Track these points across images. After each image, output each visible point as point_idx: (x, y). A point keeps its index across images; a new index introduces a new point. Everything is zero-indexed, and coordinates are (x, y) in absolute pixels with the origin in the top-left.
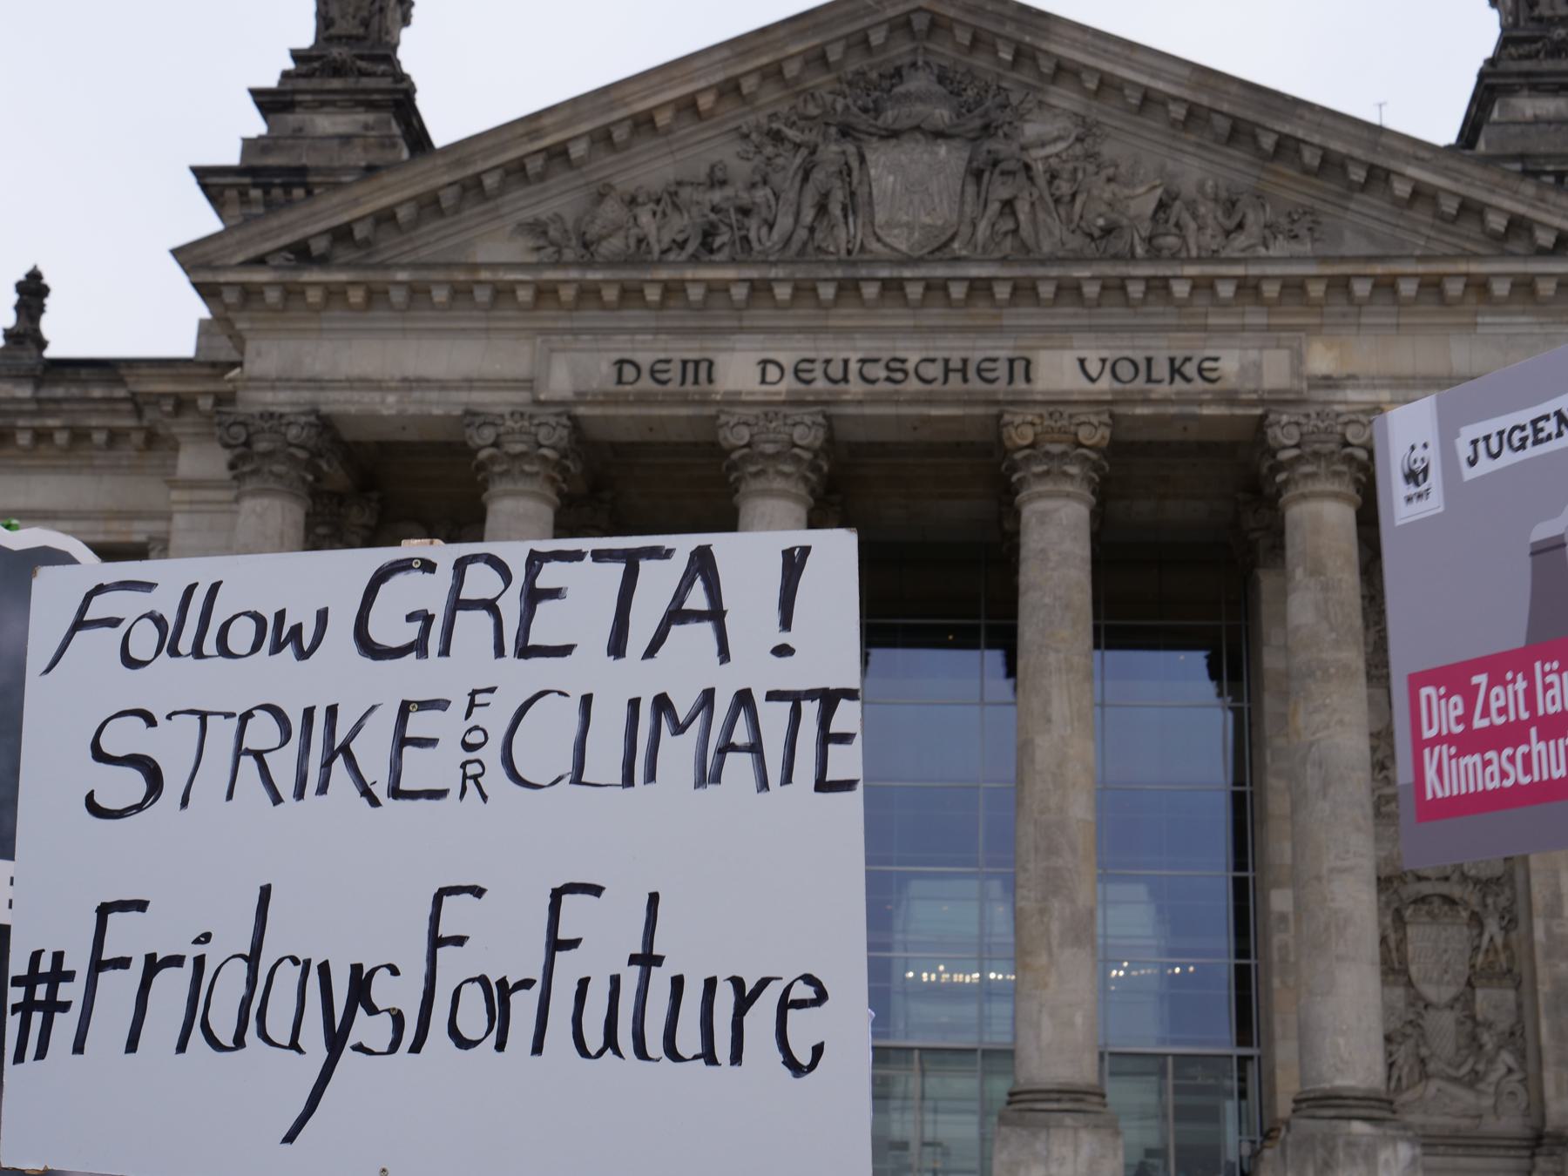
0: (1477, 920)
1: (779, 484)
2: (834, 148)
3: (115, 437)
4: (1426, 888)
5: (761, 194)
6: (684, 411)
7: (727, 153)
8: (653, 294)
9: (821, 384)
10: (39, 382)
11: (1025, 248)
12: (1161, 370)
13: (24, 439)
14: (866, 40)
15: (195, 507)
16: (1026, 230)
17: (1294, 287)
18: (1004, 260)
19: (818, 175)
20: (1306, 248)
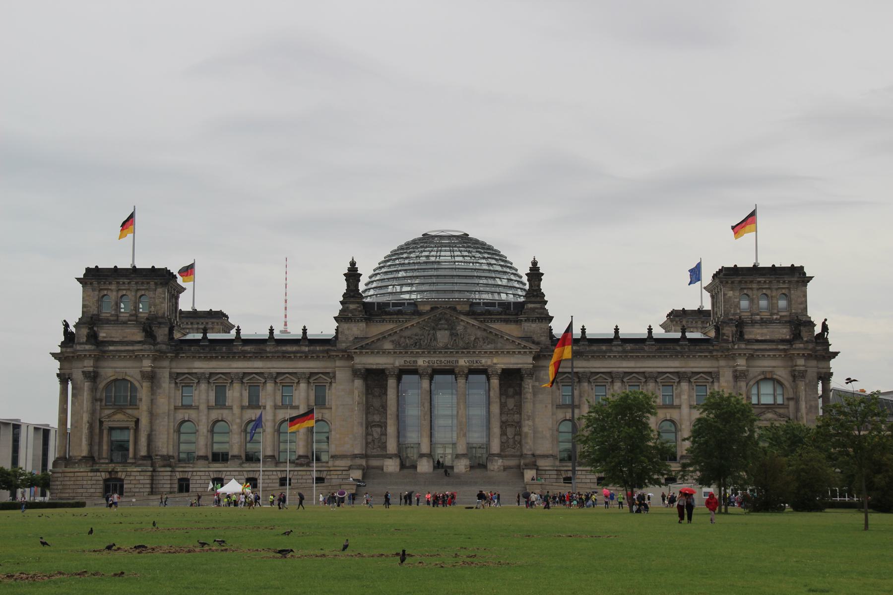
0: (516, 427)
1: (426, 378)
2: (432, 332)
3: (323, 356)
4: (509, 423)
5: (422, 337)
6: (413, 368)
7: (417, 330)
8: (409, 353)
9: (431, 364)
10: (309, 346)
11: (457, 346)
12: (475, 362)
13: (310, 357)
14: (436, 316)
16: (457, 343)
17: (491, 352)
18: (454, 349)
19: (430, 336)
20: (493, 345)
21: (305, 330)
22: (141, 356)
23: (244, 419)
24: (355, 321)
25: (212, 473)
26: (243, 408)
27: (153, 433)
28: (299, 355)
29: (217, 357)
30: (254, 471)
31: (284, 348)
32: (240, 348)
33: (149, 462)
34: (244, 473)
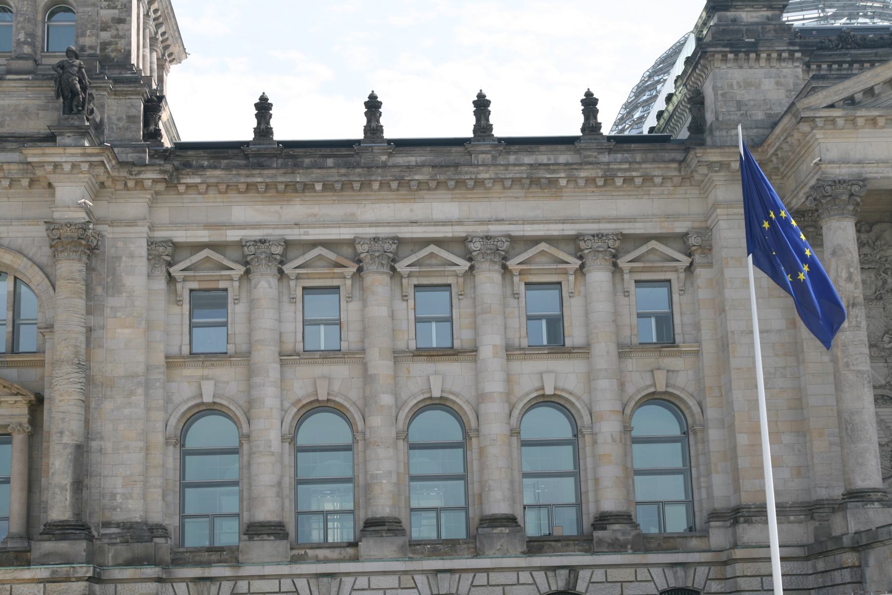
10: (610, 151)
13: (619, 182)
15: (730, 217)
21: (590, 104)
22: (50, 168)
23: (404, 396)
24: (769, 55)
25: (304, 581)
26: (398, 356)
27: (94, 444)
28: (583, 174)
29: (307, 187)
30: (451, 571)
31: (528, 159)
32: (384, 158)
33: (81, 547)
34: (417, 577)
